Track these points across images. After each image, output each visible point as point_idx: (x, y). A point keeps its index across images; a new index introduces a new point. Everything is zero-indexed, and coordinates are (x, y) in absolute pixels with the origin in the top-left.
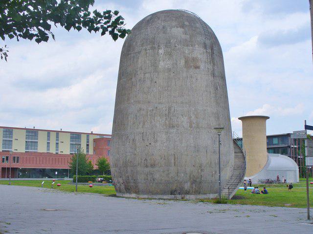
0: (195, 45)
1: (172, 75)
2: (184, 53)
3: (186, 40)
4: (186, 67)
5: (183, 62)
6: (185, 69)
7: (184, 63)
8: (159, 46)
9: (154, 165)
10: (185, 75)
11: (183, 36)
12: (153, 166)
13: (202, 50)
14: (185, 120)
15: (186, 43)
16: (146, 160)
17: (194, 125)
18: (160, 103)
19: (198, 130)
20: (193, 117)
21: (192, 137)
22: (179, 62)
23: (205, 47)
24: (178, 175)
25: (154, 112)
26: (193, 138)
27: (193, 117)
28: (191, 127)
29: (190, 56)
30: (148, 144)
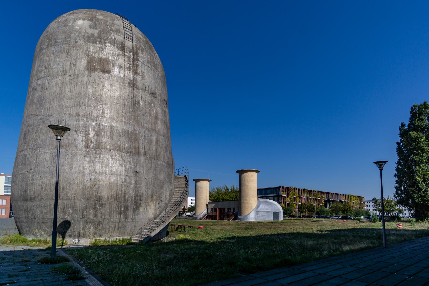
0: (105, 43)
1: (68, 78)
2: (87, 50)
3: (92, 35)
4: (88, 70)
5: (84, 63)
6: (87, 72)
7: (85, 65)
8: (56, 42)
9: (34, 198)
10: (85, 79)
11: (91, 31)
12: (32, 199)
13: (116, 51)
14: (80, 137)
15: (92, 39)
16: (26, 191)
17: (92, 145)
18: (48, 116)
19: (98, 152)
20: (92, 134)
21: (87, 159)
22: (78, 62)
23: (123, 47)
24: (64, 212)
25: (41, 127)
26: (89, 162)
27: (92, 134)
28: (87, 146)
29: (96, 55)
30: (28, 170)
